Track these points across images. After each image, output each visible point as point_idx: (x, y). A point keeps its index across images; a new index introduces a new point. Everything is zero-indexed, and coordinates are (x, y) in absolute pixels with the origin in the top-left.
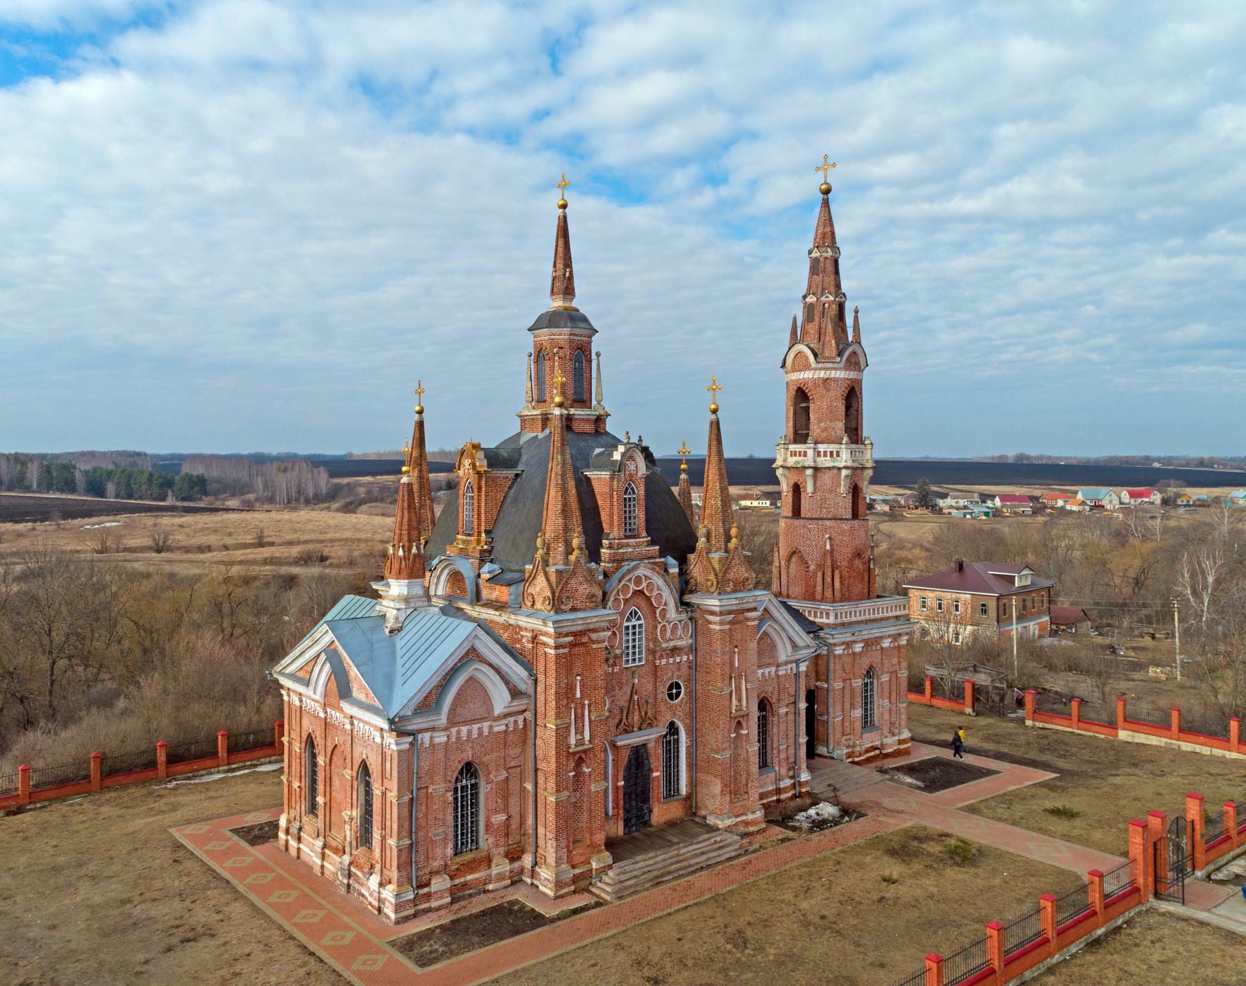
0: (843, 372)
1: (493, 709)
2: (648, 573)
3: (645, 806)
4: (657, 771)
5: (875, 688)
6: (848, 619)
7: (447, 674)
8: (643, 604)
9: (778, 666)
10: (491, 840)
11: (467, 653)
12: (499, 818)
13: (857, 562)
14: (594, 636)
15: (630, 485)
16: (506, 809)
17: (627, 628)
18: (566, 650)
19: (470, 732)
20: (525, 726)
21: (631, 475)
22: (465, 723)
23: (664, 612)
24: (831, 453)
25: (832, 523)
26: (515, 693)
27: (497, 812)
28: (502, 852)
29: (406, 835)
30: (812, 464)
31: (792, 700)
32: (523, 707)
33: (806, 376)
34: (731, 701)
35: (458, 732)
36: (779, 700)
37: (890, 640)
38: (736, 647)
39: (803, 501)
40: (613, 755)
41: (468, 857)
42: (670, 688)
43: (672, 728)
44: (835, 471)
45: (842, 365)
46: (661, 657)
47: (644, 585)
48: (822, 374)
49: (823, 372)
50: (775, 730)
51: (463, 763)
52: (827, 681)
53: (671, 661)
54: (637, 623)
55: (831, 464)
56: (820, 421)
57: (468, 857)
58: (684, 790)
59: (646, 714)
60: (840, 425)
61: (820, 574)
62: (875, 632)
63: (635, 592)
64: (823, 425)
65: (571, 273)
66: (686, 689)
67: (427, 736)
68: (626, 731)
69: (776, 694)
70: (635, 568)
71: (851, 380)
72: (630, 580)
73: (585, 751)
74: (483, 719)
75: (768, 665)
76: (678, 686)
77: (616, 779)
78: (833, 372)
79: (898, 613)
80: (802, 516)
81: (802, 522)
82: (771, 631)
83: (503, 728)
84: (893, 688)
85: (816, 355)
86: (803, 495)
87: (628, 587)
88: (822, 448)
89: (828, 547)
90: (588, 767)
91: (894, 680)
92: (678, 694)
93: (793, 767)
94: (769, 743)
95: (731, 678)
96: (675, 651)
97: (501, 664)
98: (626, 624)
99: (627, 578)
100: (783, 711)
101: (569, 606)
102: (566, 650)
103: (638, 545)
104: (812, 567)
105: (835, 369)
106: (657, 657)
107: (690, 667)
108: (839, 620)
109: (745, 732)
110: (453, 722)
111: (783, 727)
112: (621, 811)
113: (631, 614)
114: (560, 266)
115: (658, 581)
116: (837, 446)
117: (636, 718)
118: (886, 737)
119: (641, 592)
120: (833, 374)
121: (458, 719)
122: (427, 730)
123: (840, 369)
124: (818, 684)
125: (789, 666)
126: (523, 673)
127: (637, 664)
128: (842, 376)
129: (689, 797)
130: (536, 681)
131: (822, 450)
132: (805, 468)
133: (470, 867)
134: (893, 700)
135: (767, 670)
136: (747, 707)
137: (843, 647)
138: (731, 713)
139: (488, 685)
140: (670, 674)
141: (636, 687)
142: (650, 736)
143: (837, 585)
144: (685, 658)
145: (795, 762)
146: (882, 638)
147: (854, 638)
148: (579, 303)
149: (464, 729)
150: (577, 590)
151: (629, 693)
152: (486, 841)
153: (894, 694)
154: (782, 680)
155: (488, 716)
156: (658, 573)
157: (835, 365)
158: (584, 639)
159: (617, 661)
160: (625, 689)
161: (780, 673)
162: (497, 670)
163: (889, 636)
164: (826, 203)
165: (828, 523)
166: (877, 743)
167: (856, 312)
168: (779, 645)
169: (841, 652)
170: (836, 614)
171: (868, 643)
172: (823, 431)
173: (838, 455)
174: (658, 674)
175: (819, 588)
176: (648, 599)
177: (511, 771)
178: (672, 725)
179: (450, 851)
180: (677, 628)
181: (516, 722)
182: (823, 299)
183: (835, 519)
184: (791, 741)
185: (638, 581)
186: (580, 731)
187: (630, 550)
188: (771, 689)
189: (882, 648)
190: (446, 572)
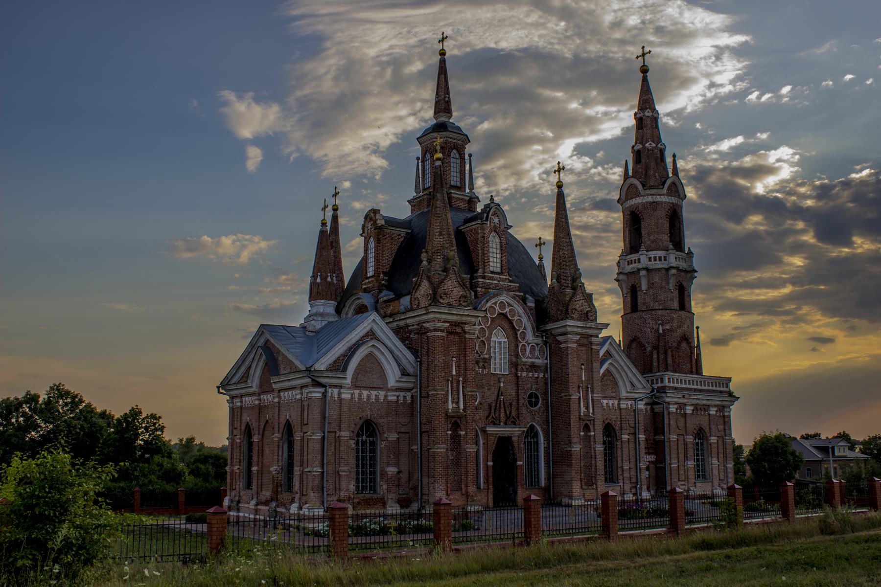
0: (666, 197)
1: (387, 383)
3: (511, 489)
4: (520, 461)
5: (705, 448)
6: (679, 385)
7: (351, 347)
8: (506, 326)
9: (620, 399)
10: (385, 487)
11: (367, 335)
12: (392, 470)
13: (684, 345)
16: (397, 464)
18: (444, 334)
19: (369, 396)
20: (412, 401)
21: (495, 226)
22: (365, 388)
23: (524, 334)
25: (664, 313)
26: (404, 373)
27: (388, 465)
28: (394, 498)
29: (319, 465)
30: (644, 266)
31: (632, 431)
32: (411, 385)
33: (636, 202)
34: (580, 407)
35: (360, 395)
36: (621, 428)
37: (715, 409)
38: (583, 364)
39: (639, 298)
40: (483, 440)
41: (367, 495)
42: (530, 396)
43: (532, 432)
44: (664, 272)
45: (665, 190)
46: (522, 370)
47: (507, 310)
48: (650, 199)
49: (650, 197)
50: (619, 453)
51: (362, 421)
52: (663, 434)
53: (530, 375)
55: (660, 266)
56: (649, 234)
57: (367, 495)
58: (543, 483)
59: (510, 413)
60: (666, 237)
61: (655, 353)
62: (703, 400)
64: (652, 237)
65: (449, 98)
66: (543, 400)
67: (336, 391)
68: (495, 424)
69: (619, 423)
71: (672, 203)
72: (495, 303)
73: (460, 418)
74: (380, 389)
75: (612, 398)
76: (536, 397)
78: (658, 197)
79: (722, 389)
80: (639, 309)
81: (639, 314)
82: (612, 369)
83: (395, 398)
84: (721, 450)
85: (644, 186)
86: (639, 293)
87: (495, 309)
88: (652, 254)
89: (661, 331)
91: (720, 443)
92: (536, 403)
93: (635, 485)
94: (614, 463)
95: (579, 387)
96: (533, 367)
97: (393, 348)
99: (493, 301)
101: (446, 301)
102: (444, 334)
104: (649, 349)
105: (659, 195)
106: (519, 369)
107: (546, 384)
109: (592, 433)
110: (355, 385)
111: (625, 451)
112: (491, 487)
114: (441, 93)
115: (518, 308)
116: (664, 252)
117: (502, 415)
118: (716, 489)
119: (504, 315)
120: (658, 199)
121: (358, 384)
122: (335, 386)
123: (663, 195)
124: (657, 437)
125: (629, 403)
126: (411, 358)
128: (664, 200)
129: (547, 489)
130: (420, 362)
131: (653, 256)
132: (639, 270)
133: (368, 503)
134: (721, 461)
135: (611, 402)
136: (593, 413)
137: (676, 406)
138: (580, 413)
139: (384, 362)
140: (529, 386)
141: (502, 390)
142: (514, 431)
144: (542, 375)
145: (637, 482)
147: (685, 401)
149: (365, 393)
151: (496, 393)
152: (383, 488)
153: (721, 456)
154: (623, 412)
155: (383, 386)
156: (518, 301)
157: (659, 191)
158: (459, 330)
159: (486, 365)
160: (493, 389)
161: (622, 406)
162: (391, 352)
163: (715, 406)
164: (645, 80)
165: (659, 313)
166: (709, 493)
167: (674, 156)
169: (674, 410)
170: (669, 379)
171: (696, 408)
172: (652, 242)
173: (665, 259)
174: (520, 383)
175: (655, 364)
176: (510, 322)
177: (401, 435)
178: (532, 427)
179: (352, 487)
180: (534, 349)
181: (405, 397)
182: (647, 145)
184: (633, 465)
188: (614, 418)
189: (709, 415)
190: (353, 307)
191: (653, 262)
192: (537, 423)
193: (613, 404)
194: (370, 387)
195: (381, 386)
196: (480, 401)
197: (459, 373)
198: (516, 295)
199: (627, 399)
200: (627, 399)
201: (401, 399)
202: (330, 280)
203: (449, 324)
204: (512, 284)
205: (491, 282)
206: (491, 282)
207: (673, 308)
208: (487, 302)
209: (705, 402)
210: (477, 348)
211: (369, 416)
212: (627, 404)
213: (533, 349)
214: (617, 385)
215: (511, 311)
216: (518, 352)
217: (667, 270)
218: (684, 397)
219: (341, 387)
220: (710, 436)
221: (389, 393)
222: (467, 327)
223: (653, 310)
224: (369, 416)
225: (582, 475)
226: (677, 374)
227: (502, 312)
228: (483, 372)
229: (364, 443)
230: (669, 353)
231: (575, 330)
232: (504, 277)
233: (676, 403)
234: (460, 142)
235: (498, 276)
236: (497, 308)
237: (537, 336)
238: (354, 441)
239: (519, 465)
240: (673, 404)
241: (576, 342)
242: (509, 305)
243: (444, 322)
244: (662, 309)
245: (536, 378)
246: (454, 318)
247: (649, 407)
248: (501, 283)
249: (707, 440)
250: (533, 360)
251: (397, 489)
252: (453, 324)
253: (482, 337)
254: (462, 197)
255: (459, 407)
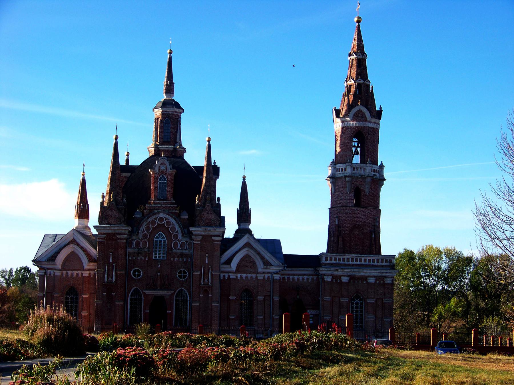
2: (167, 216)
9: (258, 273)
14: (118, 236)
15: (163, 176)
17: (156, 241)
18: (103, 240)
19: (72, 274)
22: (70, 270)
23: (176, 237)
24: (342, 169)
35: (67, 273)
37: (374, 279)
38: (207, 253)
40: (144, 298)
44: (344, 179)
46: (174, 257)
47: (165, 222)
53: (180, 259)
54: (162, 240)
63: (158, 225)
67: (52, 272)
70: (158, 213)
72: (156, 219)
76: (185, 272)
77: (145, 309)
87: (156, 222)
89: (337, 223)
90: (114, 293)
96: (182, 255)
98: (155, 239)
99: (154, 217)
100: (261, 298)
102: (103, 240)
103: (167, 204)
108: (329, 262)
109: (210, 295)
113: (159, 235)
115: (173, 221)
125: (266, 276)
127: (162, 258)
131: (338, 168)
135: (249, 276)
143: (340, 244)
146: (368, 276)
147: (341, 273)
148: (177, 97)
149: (70, 272)
150: (111, 216)
156: (171, 216)
165: (339, 209)
168: (257, 263)
173: (345, 170)
176: (168, 229)
183: (342, 207)
185: (161, 219)
186: (110, 275)
187: (159, 205)
191: (338, 172)
192: (185, 288)
193: (251, 277)
194: (73, 269)
195: (80, 268)
196: (142, 276)
197: (113, 262)
198: (169, 212)
199: (263, 273)
200: (263, 273)
201: (92, 276)
202: (82, 207)
203: (106, 235)
204: (171, 206)
205: (156, 205)
206: (156, 205)
207: (348, 206)
208: (148, 218)
209: (362, 274)
210: (141, 245)
211: (72, 284)
212: (264, 277)
213: (183, 245)
214: (256, 263)
215: (167, 222)
216: (172, 246)
217: (345, 177)
218: (337, 270)
219: (55, 269)
220: (367, 298)
221: (83, 272)
222: (118, 236)
223: (336, 207)
224: (72, 284)
225: (200, 320)
226: (335, 254)
227: (161, 223)
228: (145, 259)
229: (72, 298)
230: (341, 239)
231: (199, 233)
232: (167, 201)
233: (331, 275)
234: (172, 113)
235: (162, 201)
236: (157, 222)
237: (185, 237)
238: (63, 297)
239: (169, 313)
240: (329, 275)
241: (201, 240)
242: (166, 219)
243: (104, 234)
244: (340, 207)
245: (185, 261)
246: (110, 232)
247: (315, 277)
248: (163, 205)
249: (365, 301)
250: (182, 251)
251: (88, 323)
252: (108, 234)
253: (145, 239)
254: (167, 149)
255: (112, 280)
